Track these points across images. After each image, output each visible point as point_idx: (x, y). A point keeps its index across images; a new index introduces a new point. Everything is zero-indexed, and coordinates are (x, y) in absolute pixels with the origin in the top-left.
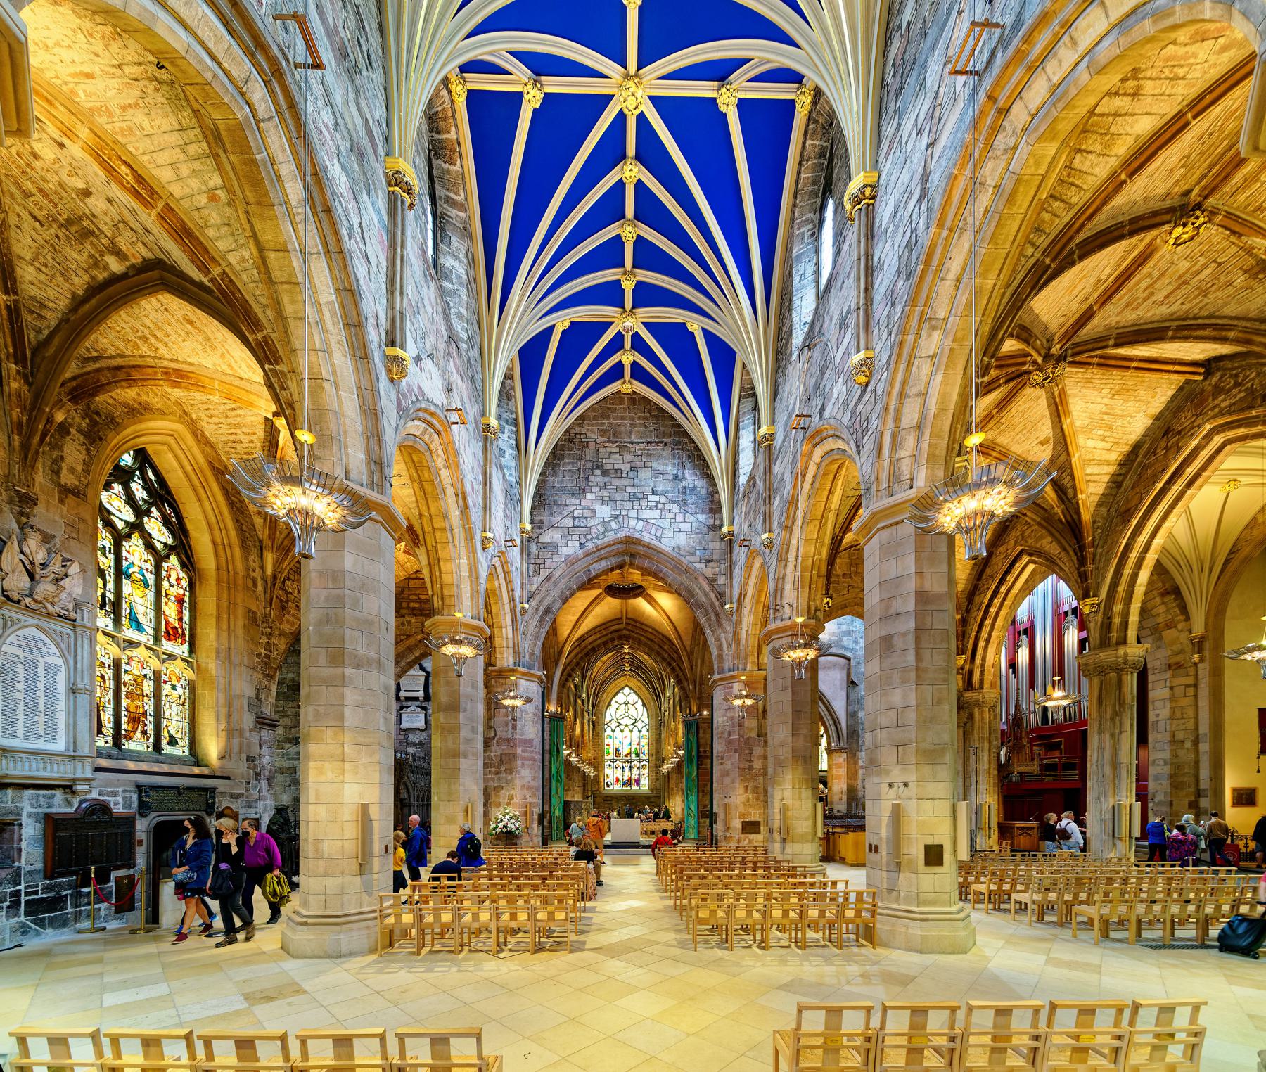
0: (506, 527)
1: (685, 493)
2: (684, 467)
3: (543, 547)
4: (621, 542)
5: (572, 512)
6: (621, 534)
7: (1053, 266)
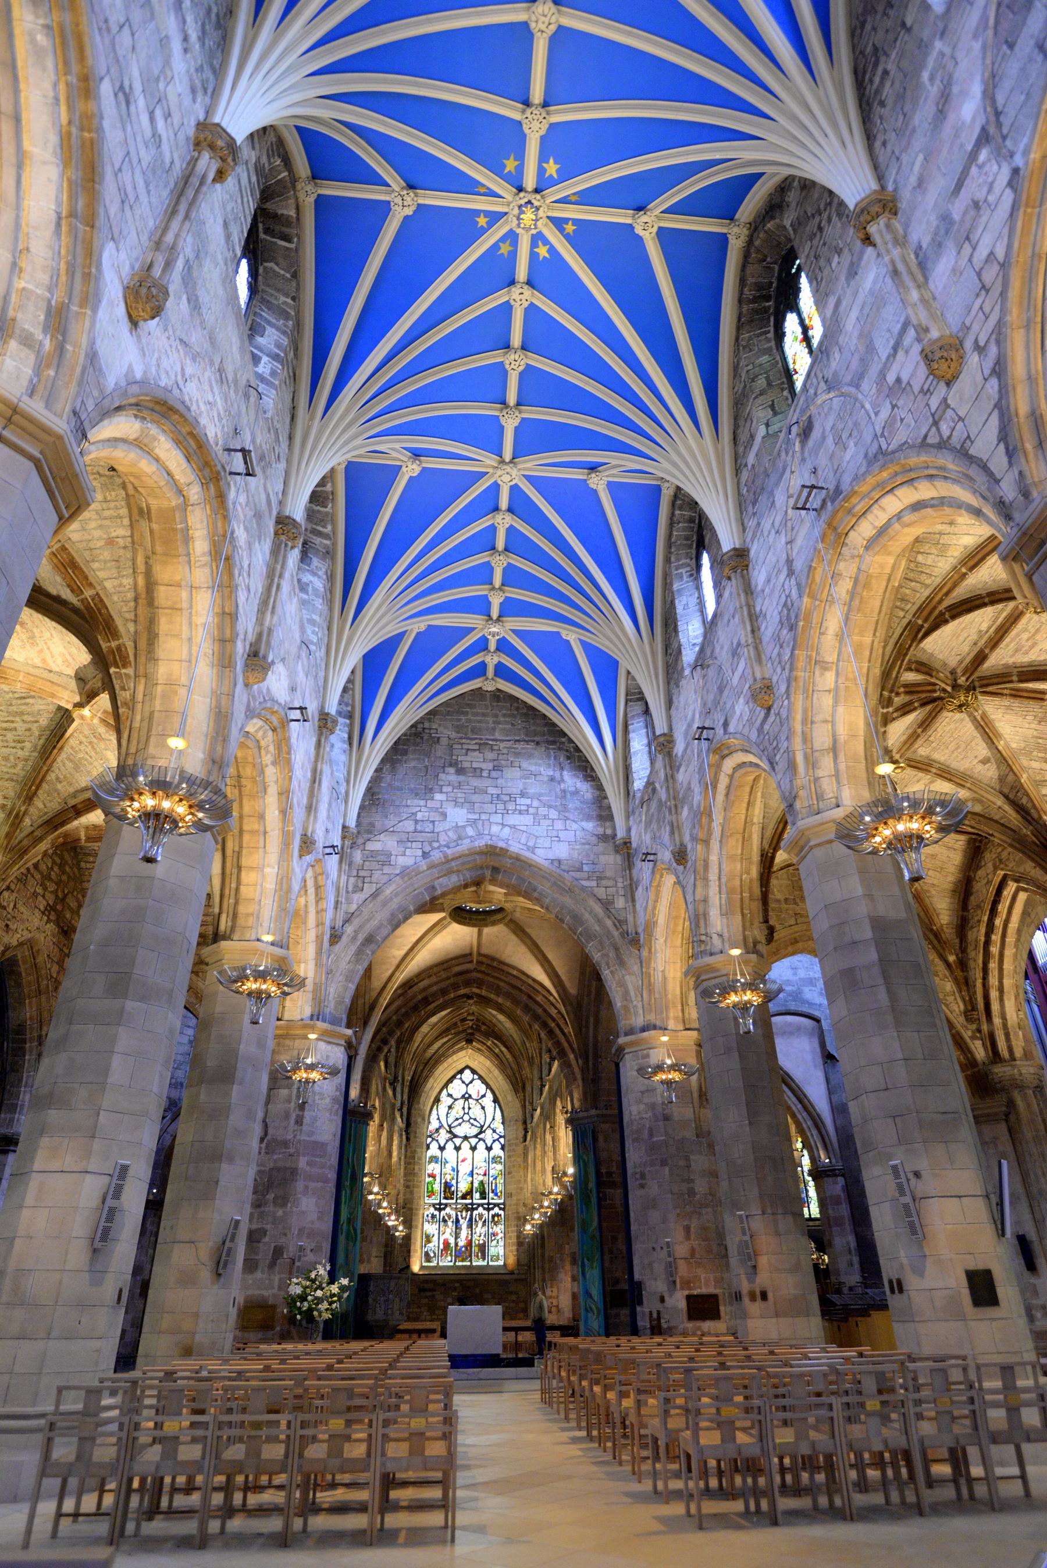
0: (327, 831)
1: (564, 797)
2: (562, 769)
3: (373, 855)
4: (481, 853)
5: (415, 814)
6: (480, 843)
7: (926, 625)
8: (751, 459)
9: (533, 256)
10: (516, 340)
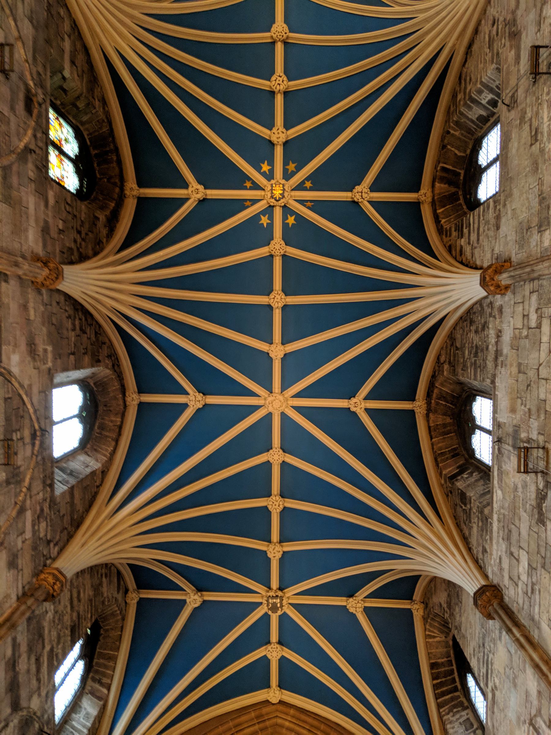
8: (67, 45)
9: (271, 163)
10: (279, 100)
